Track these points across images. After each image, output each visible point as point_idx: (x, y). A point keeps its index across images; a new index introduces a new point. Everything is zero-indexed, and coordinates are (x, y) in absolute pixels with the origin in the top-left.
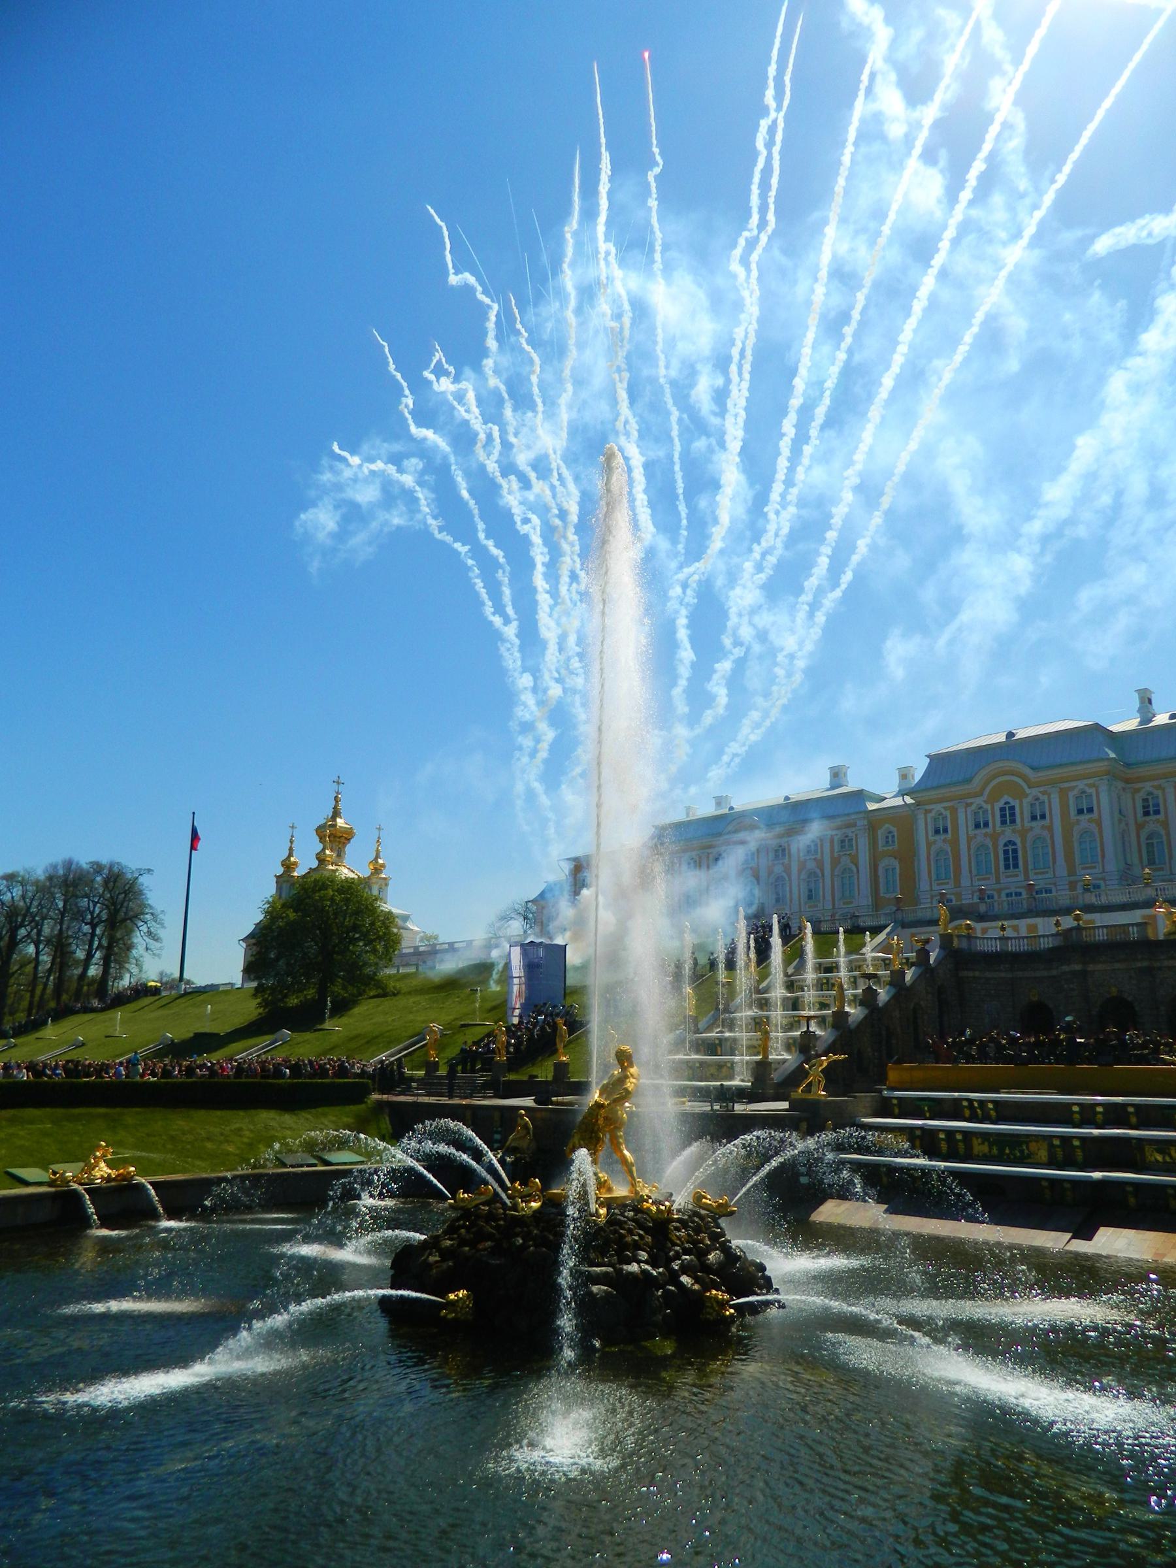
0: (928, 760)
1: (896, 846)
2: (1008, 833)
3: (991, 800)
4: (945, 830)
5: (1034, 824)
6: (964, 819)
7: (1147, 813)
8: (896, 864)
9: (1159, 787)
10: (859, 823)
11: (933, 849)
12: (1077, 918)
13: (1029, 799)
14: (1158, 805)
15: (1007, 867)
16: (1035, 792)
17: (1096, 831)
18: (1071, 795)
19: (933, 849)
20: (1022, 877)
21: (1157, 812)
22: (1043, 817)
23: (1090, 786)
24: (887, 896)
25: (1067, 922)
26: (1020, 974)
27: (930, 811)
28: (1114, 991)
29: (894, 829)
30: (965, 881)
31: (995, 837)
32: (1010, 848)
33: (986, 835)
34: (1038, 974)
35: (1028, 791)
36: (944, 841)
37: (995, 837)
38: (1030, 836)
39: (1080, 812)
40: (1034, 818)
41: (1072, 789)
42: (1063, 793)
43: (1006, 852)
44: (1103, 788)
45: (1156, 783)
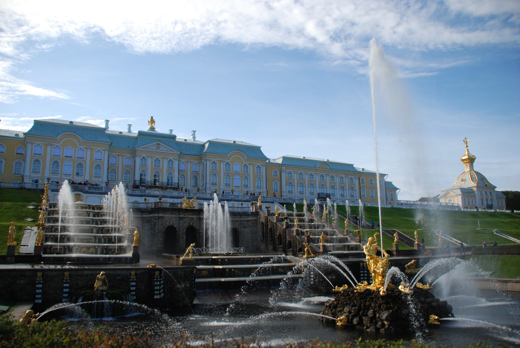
8: (4, 161)
9: (118, 155)
11: (33, 160)
12: (160, 199)
16: (81, 147)
23: (102, 149)
25: (157, 200)
35: (78, 146)
41: (96, 149)
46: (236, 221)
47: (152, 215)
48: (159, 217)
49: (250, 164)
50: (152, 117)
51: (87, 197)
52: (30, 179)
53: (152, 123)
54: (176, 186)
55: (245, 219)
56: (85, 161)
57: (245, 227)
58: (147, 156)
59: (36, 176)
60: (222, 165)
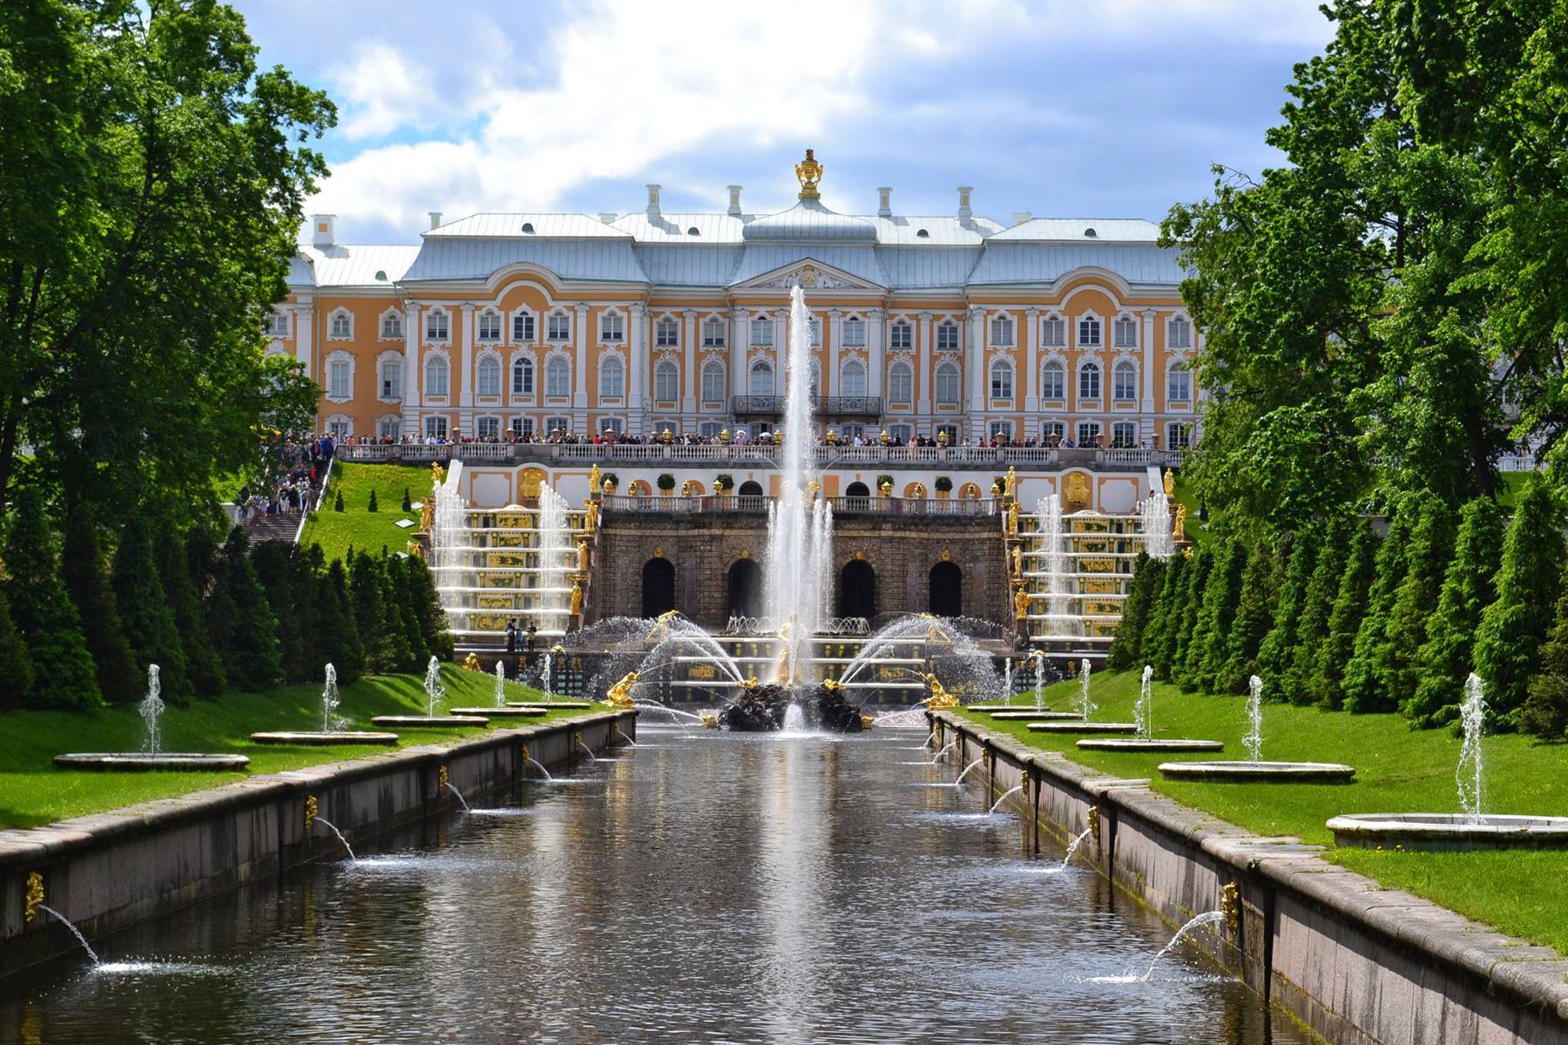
0: (422, 241)
1: (352, 339)
2: (523, 350)
3: (507, 305)
4: (443, 334)
5: (554, 343)
6: (470, 325)
7: (661, 342)
9: (680, 315)
10: (300, 300)
13: (552, 313)
14: (674, 333)
15: (517, 388)
16: (559, 306)
17: (623, 361)
18: (600, 315)
19: (427, 356)
20: (534, 403)
21: (673, 342)
22: (565, 335)
24: (335, 400)
26: (647, 532)
27: (427, 308)
28: (745, 555)
29: (351, 317)
30: (466, 399)
31: (507, 352)
32: (523, 366)
33: (495, 347)
34: (665, 533)
35: (550, 303)
36: (443, 347)
37: (507, 352)
38: (548, 356)
39: (606, 336)
40: (553, 335)
42: (592, 313)
43: (518, 371)
44: (636, 315)
45: (679, 310)
46: (952, 541)
47: (696, 532)
48: (713, 538)
49: (1138, 314)
50: (809, 152)
51: (557, 476)
52: (421, 413)
53: (809, 175)
54: (871, 410)
55: (977, 536)
56: (573, 351)
57: (975, 559)
58: (772, 314)
59: (439, 407)
60: (1034, 327)
